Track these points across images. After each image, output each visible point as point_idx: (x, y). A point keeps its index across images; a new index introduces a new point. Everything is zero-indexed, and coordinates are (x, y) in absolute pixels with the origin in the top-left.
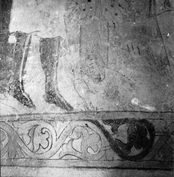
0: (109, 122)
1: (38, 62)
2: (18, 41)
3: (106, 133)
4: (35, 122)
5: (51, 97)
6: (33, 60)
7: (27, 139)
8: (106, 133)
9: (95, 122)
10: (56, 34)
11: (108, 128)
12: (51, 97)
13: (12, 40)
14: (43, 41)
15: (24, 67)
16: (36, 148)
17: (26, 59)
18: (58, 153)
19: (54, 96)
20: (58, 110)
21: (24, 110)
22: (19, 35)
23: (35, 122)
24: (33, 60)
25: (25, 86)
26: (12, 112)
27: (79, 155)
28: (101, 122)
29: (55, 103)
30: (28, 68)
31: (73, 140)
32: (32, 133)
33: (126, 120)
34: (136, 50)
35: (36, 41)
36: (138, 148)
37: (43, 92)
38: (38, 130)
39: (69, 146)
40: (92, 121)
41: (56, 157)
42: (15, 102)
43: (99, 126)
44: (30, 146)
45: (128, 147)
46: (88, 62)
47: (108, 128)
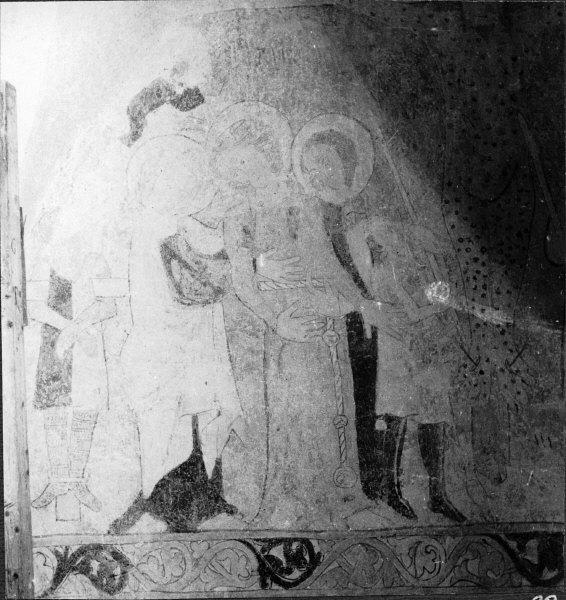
0: (514, 536)
1: (417, 457)
2: (388, 427)
4: (419, 538)
6: (410, 454)
9: (496, 537)
10: (441, 419)
11: (513, 544)
12: (437, 503)
13: (380, 425)
14: (423, 427)
15: (398, 465)
16: (419, 572)
17: (400, 452)
18: (449, 578)
19: (441, 503)
20: (447, 522)
21: (402, 521)
22: (389, 419)
23: (419, 538)
24: (410, 454)
25: (402, 489)
26: (387, 525)
27: (475, 579)
28: (503, 536)
29: (442, 512)
30: (405, 464)
31: (467, 560)
32: (413, 551)
33: (535, 535)
34: (547, 443)
35: (412, 427)
36: (551, 569)
37: (425, 498)
38: (421, 548)
39: (463, 569)
40: (493, 536)
41: (446, 583)
43: (500, 540)
44: (411, 570)
45: (540, 568)
46: (484, 457)
47: (513, 544)
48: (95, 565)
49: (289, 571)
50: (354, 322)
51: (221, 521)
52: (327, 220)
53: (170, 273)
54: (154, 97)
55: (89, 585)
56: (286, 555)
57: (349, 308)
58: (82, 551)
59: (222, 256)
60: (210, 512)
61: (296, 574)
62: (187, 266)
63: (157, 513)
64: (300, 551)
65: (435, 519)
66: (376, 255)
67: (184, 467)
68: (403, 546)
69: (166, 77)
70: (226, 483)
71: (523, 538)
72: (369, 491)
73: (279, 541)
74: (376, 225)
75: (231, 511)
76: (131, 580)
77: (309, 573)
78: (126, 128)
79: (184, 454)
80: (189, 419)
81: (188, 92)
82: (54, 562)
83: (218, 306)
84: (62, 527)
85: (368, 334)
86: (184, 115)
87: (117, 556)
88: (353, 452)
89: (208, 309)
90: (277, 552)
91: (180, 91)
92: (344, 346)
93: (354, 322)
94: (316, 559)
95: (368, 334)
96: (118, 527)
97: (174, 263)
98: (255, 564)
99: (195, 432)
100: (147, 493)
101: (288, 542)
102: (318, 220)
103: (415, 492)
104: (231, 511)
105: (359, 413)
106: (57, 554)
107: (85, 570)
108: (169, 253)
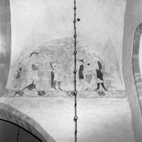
0: (68, 92)
1: (58, 84)
3: (67, 93)
5: (59, 88)
7: (55, 94)
8: (67, 93)
9: (66, 92)
14: (59, 82)
22: (55, 81)
24: (57, 84)
33: (70, 92)
42: (54, 89)
43: (66, 92)
45: (71, 95)
47: (68, 92)
48: (20, 93)
49: (42, 94)
50: (52, 72)
51: (35, 89)
52: (50, 63)
53: (32, 67)
54: (33, 53)
55: (19, 95)
56: (42, 92)
57: (51, 71)
58: (19, 92)
59: (38, 66)
60: (34, 88)
61: (42, 94)
62: (34, 67)
63: (27, 88)
64: (43, 92)
65: (59, 90)
66: (55, 66)
67: (31, 84)
68: (55, 92)
69: (35, 52)
70: (36, 86)
71: (69, 92)
72: (52, 87)
73: (41, 91)
74: (55, 64)
75: (36, 88)
76: (24, 95)
77: (44, 94)
78: (30, 55)
79: (32, 83)
80: (33, 80)
81: (37, 53)
82: (15, 92)
83: (37, 70)
84: (17, 89)
85: (54, 73)
86: (36, 55)
87: (23, 92)
88: (50, 84)
89: (36, 71)
90: (41, 92)
91: (36, 53)
92: (51, 74)
93: (52, 72)
94: (45, 93)
95: (54, 73)
96: (23, 90)
97: (33, 67)
98: (38, 93)
99: (33, 81)
100: (27, 87)
101: (42, 91)
102: (49, 63)
103: (57, 87)
104: (36, 88)
105: (52, 80)
106: (16, 92)
107: (19, 93)
108: (33, 66)
